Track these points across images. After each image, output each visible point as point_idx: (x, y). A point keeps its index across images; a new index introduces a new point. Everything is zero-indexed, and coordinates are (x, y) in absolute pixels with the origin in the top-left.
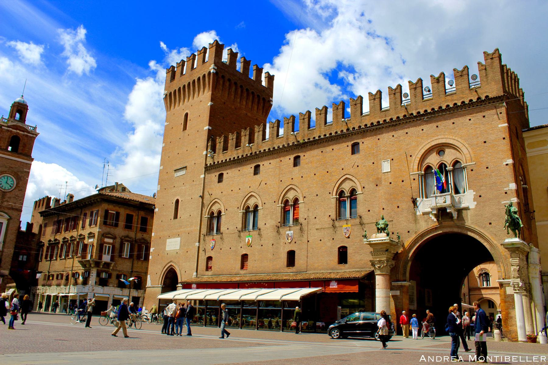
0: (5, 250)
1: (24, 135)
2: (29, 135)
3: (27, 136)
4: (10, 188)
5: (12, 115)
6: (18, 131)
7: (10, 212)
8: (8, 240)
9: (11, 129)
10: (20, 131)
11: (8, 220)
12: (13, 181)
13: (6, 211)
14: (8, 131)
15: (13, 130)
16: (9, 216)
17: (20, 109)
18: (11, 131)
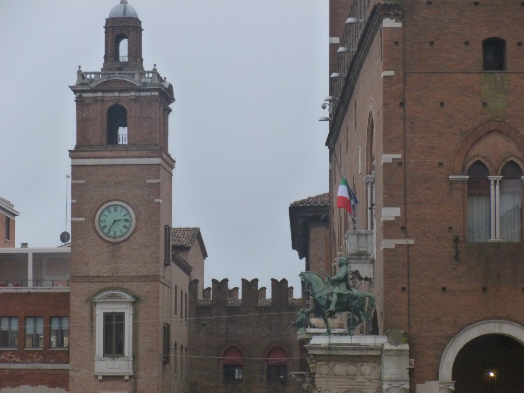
0: (141, 373)
1: (130, 100)
2: (143, 94)
3: (137, 100)
4: (124, 230)
5: (111, 53)
6: (116, 94)
7: (135, 287)
8: (141, 351)
9: (100, 94)
10: (121, 91)
11: (134, 304)
12: (129, 213)
13: (126, 285)
14: (96, 100)
15: (106, 95)
16: (134, 297)
17: (123, 29)
18: (102, 100)
